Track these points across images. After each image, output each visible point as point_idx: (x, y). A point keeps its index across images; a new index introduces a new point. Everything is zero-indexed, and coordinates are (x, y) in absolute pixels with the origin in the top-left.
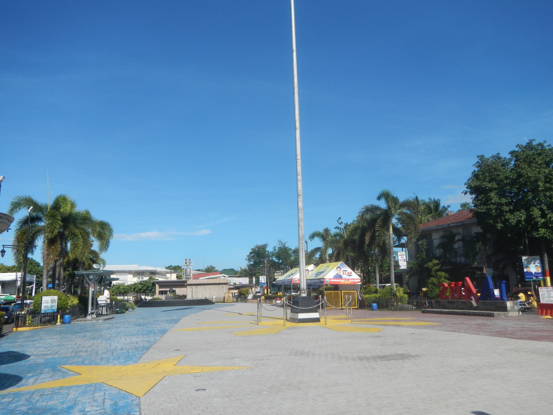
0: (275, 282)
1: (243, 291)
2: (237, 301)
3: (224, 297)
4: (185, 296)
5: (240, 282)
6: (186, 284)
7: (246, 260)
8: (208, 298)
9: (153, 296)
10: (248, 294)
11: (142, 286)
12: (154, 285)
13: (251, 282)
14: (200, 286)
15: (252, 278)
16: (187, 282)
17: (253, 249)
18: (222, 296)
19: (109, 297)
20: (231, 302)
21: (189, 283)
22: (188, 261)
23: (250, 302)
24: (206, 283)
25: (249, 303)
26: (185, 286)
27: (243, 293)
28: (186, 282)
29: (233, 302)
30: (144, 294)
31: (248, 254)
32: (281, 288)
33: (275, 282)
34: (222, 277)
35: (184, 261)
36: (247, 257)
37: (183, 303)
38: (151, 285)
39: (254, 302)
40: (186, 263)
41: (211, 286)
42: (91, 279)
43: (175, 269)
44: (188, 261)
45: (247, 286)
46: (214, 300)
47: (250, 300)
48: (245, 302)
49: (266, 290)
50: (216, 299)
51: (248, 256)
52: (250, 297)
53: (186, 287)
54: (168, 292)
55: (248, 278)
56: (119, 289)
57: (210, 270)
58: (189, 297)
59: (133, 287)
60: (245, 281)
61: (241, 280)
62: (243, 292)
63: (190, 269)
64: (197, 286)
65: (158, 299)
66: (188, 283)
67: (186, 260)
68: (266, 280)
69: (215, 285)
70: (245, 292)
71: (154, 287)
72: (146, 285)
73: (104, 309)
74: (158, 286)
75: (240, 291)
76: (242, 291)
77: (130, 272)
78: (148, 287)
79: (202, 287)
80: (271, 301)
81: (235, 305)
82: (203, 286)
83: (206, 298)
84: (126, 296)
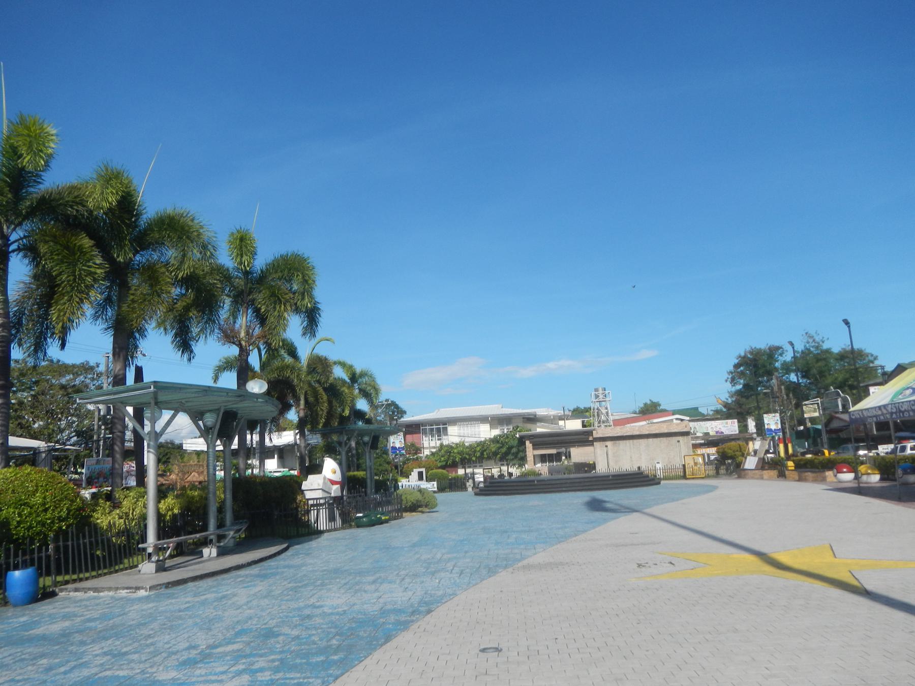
0: (802, 428)
1: (731, 450)
2: (718, 473)
3: (684, 466)
4: (593, 466)
5: (718, 430)
6: (591, 439)
7: (726, 381)
8: (644, 467)
9: (521, 466)
10: (743, 455)
11: (498, 445)
12: (522, 441)
13: (744, 428)
14: (625, 441)
15: (746, 420)
17: (740, 357)
18: (678, 462)
19: (338, 477)
20: (703, 478)
21: (598, 436)
22: (601, 392)
23: (753, 478)
24: (638, 433)
25: (749, 478)
26: (591, 443)
27: (730, 455)
28: (590, 433)
29: (708, 477)
30: (505, 463)
31: (731, 368)
32: (819, 440)
33: (802, 428)
34: (674, 420)
35: (593, 393)
36: (728, 376)
37: (577, 485)
38: (515, 443)
39: (765, 477)
40: (597, 396)
41: (651, 440)
42: (211, 428)
43: (578, 413)
44: (601, 392)
45: (733, 439)
46: (660, 474)
47: (754, 472)
48: (740, 477)
49: (781, 446)
50: (664, 469)
51: (732, 373)
52: (750, 463)
54: (564, 458)
55: (736, 421)
56: (452, 454)
57: (650, 410)
58: (602, 468)
59: (478, 449)
60: (730, 427)
61: (721, 426)
62: (730, 451)
63: (607, 408)
64: (617, 442)
65: (533, 473)
66: (595, 435)
67: (596, 390)
68: (779, 422)
69: (660, 437)
70: (734, 451)
71: (523, 447)
72: (507, 443)
73: (323, 514)
75: (721, 450)
76: (726, 450)
77: (483, 419)
78: (510, 448)
79: (628, 444)
80: (818, 474)
81: (715, 488)
82: (631, 441)
83: (639, 468)
84: (469, 467)
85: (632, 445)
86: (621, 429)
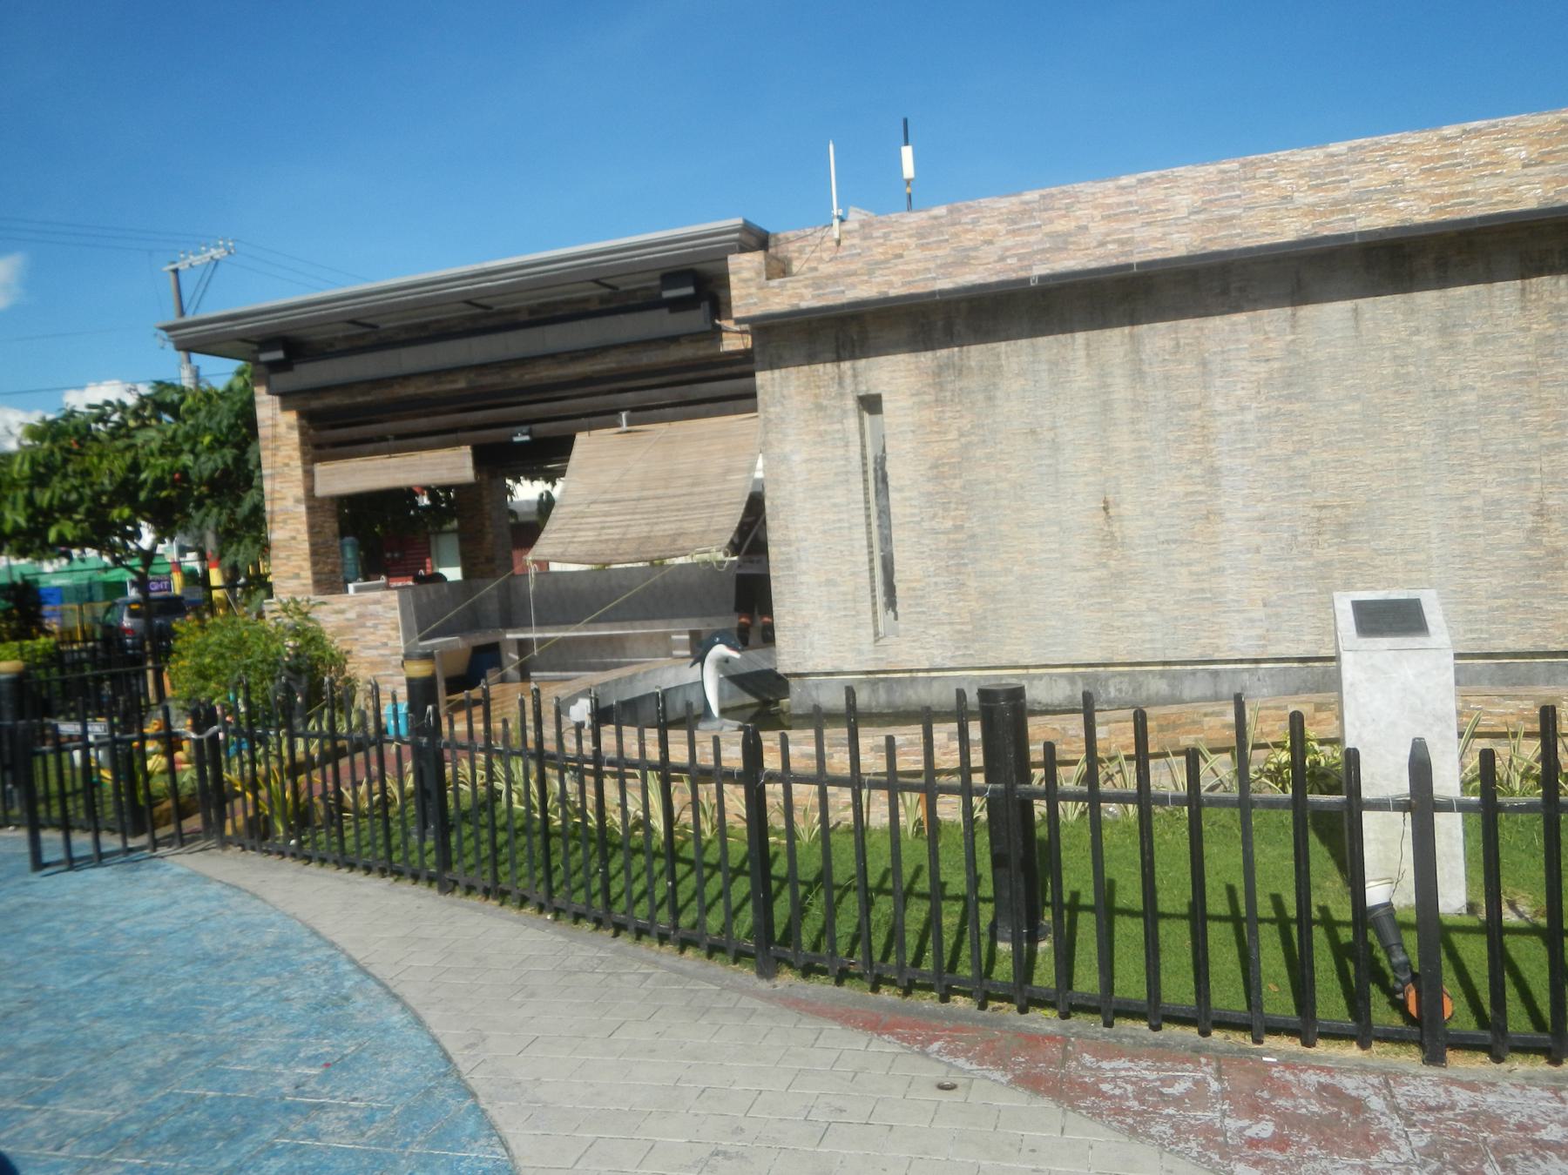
6: (734, 342)
14: (1048, 346)
16: (744, 269)
21: (782, 298)
53: (745, 400)
64: (976, 353)
74: (291, 417)
79: (1081, 377)
82: (1115, 340)
85: (1120, 389)
86: (1012, 220)
